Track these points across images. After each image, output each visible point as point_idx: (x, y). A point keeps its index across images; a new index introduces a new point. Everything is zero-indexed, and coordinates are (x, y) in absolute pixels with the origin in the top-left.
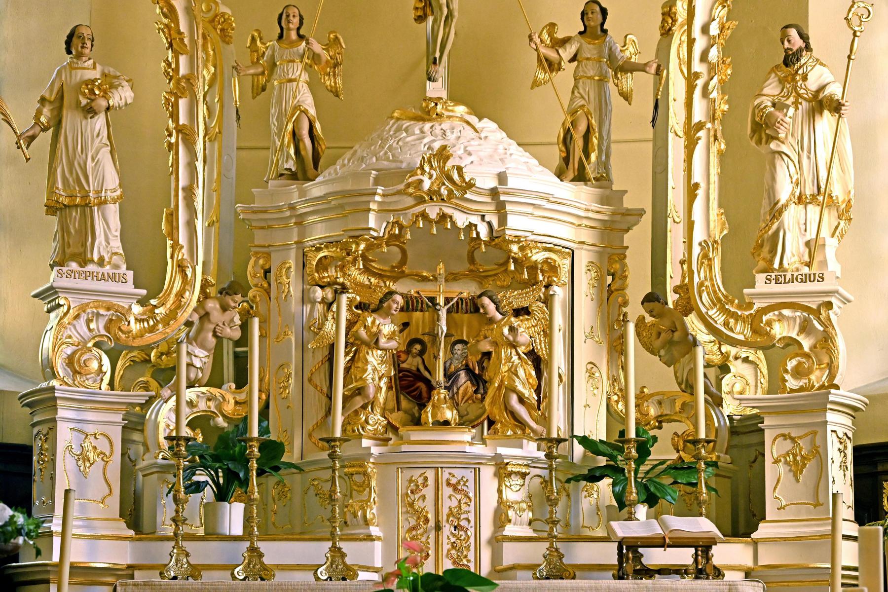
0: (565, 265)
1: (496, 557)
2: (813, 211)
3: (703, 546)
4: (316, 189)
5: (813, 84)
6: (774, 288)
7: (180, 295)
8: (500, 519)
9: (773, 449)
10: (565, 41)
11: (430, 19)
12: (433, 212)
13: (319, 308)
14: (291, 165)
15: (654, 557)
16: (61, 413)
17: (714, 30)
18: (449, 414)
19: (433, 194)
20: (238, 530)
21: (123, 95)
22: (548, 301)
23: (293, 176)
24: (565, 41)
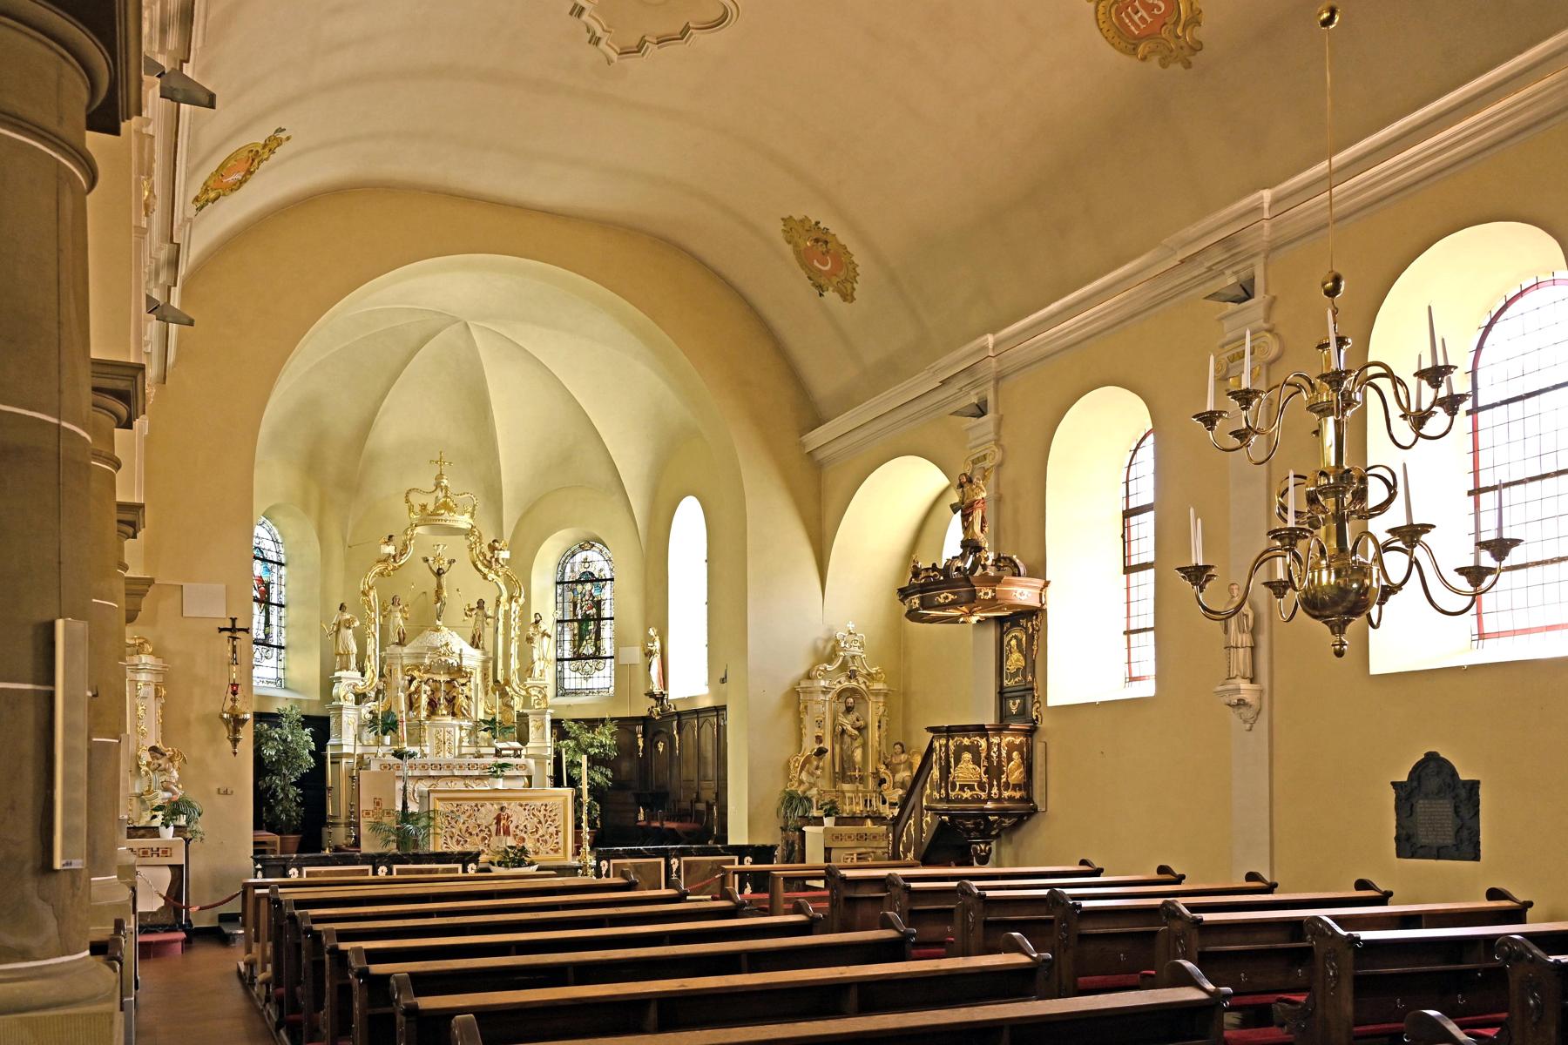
0: (474, 671)
1: (460, 751)
2: (543, 662)
3: (515, 750)
4: (406, 650)
5: (542, 629)
6: (532, 682)
7: (373, 679)
8: (461, 741)
9: (531, 724)
10: (473, 609)
11: (439, 604)
12: (443, 659)
13: (407, 682)
14: (397, 641)
15: (503, 752)
16: (343, 711)
17: (517, 613)
18: (445, 712)
19: (444, 654)
20: (389, 744)
21: (357, 624)
22: (470, 681)
23: (397, 644)
24: (472, 610)
